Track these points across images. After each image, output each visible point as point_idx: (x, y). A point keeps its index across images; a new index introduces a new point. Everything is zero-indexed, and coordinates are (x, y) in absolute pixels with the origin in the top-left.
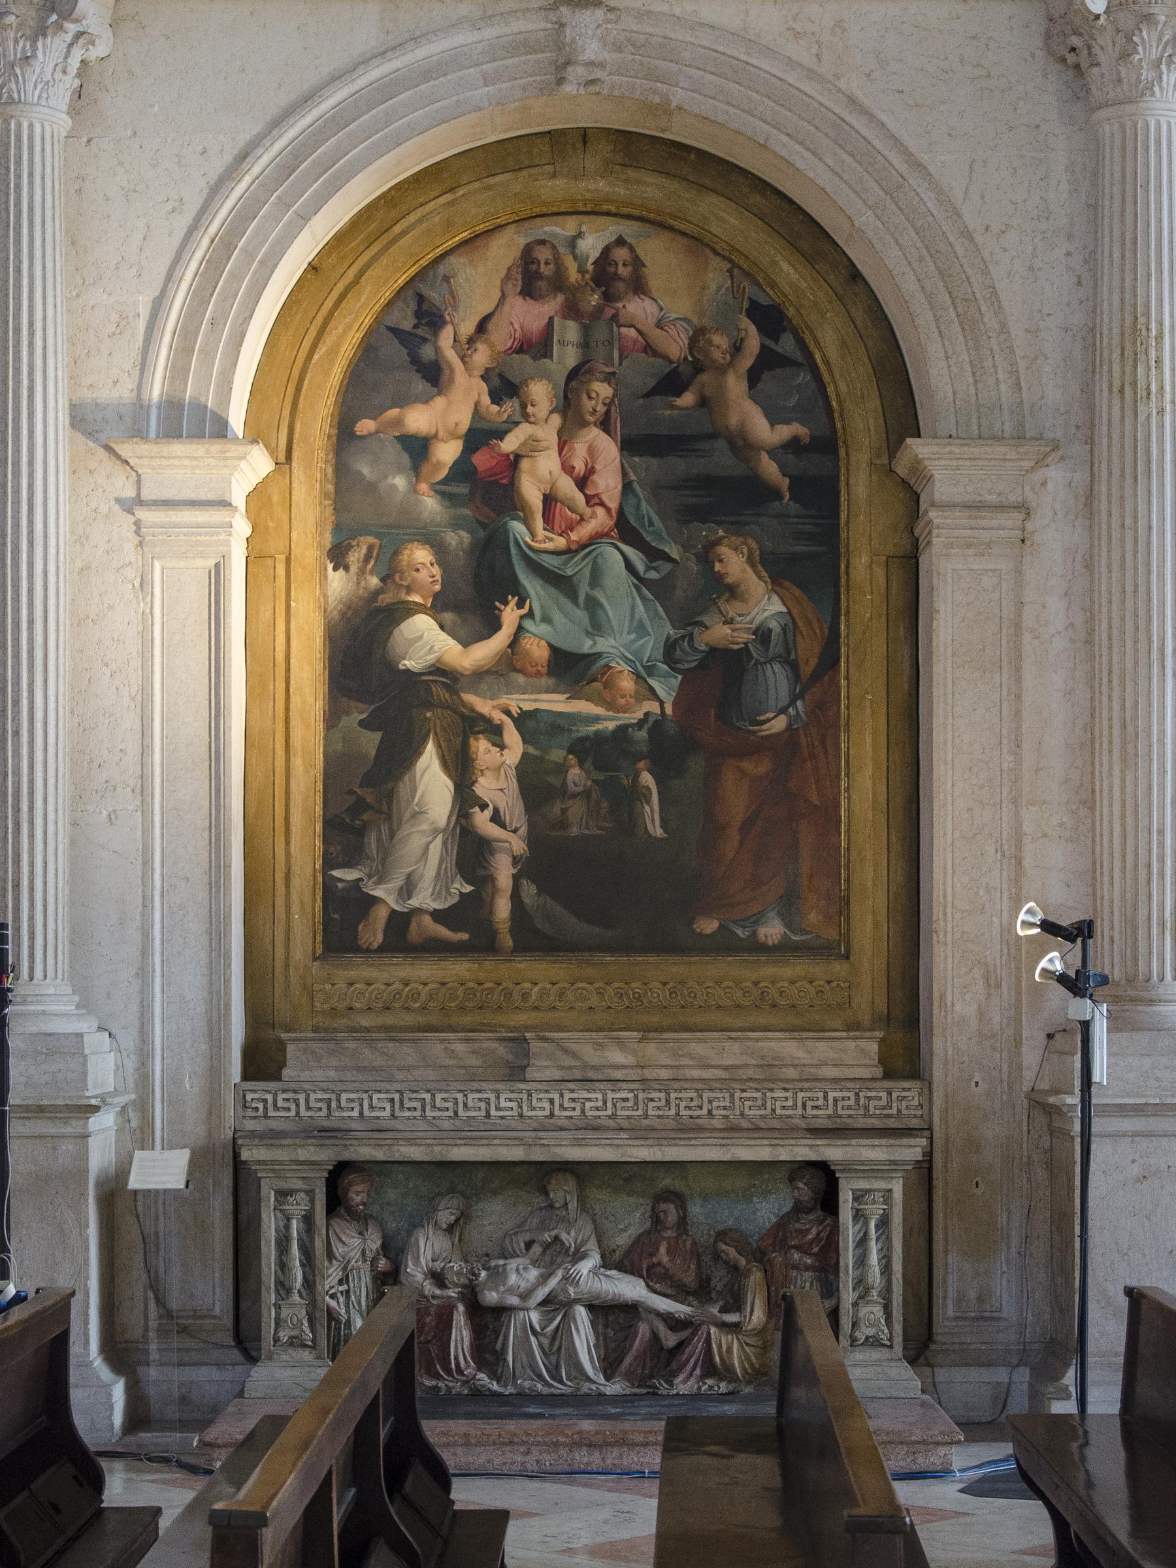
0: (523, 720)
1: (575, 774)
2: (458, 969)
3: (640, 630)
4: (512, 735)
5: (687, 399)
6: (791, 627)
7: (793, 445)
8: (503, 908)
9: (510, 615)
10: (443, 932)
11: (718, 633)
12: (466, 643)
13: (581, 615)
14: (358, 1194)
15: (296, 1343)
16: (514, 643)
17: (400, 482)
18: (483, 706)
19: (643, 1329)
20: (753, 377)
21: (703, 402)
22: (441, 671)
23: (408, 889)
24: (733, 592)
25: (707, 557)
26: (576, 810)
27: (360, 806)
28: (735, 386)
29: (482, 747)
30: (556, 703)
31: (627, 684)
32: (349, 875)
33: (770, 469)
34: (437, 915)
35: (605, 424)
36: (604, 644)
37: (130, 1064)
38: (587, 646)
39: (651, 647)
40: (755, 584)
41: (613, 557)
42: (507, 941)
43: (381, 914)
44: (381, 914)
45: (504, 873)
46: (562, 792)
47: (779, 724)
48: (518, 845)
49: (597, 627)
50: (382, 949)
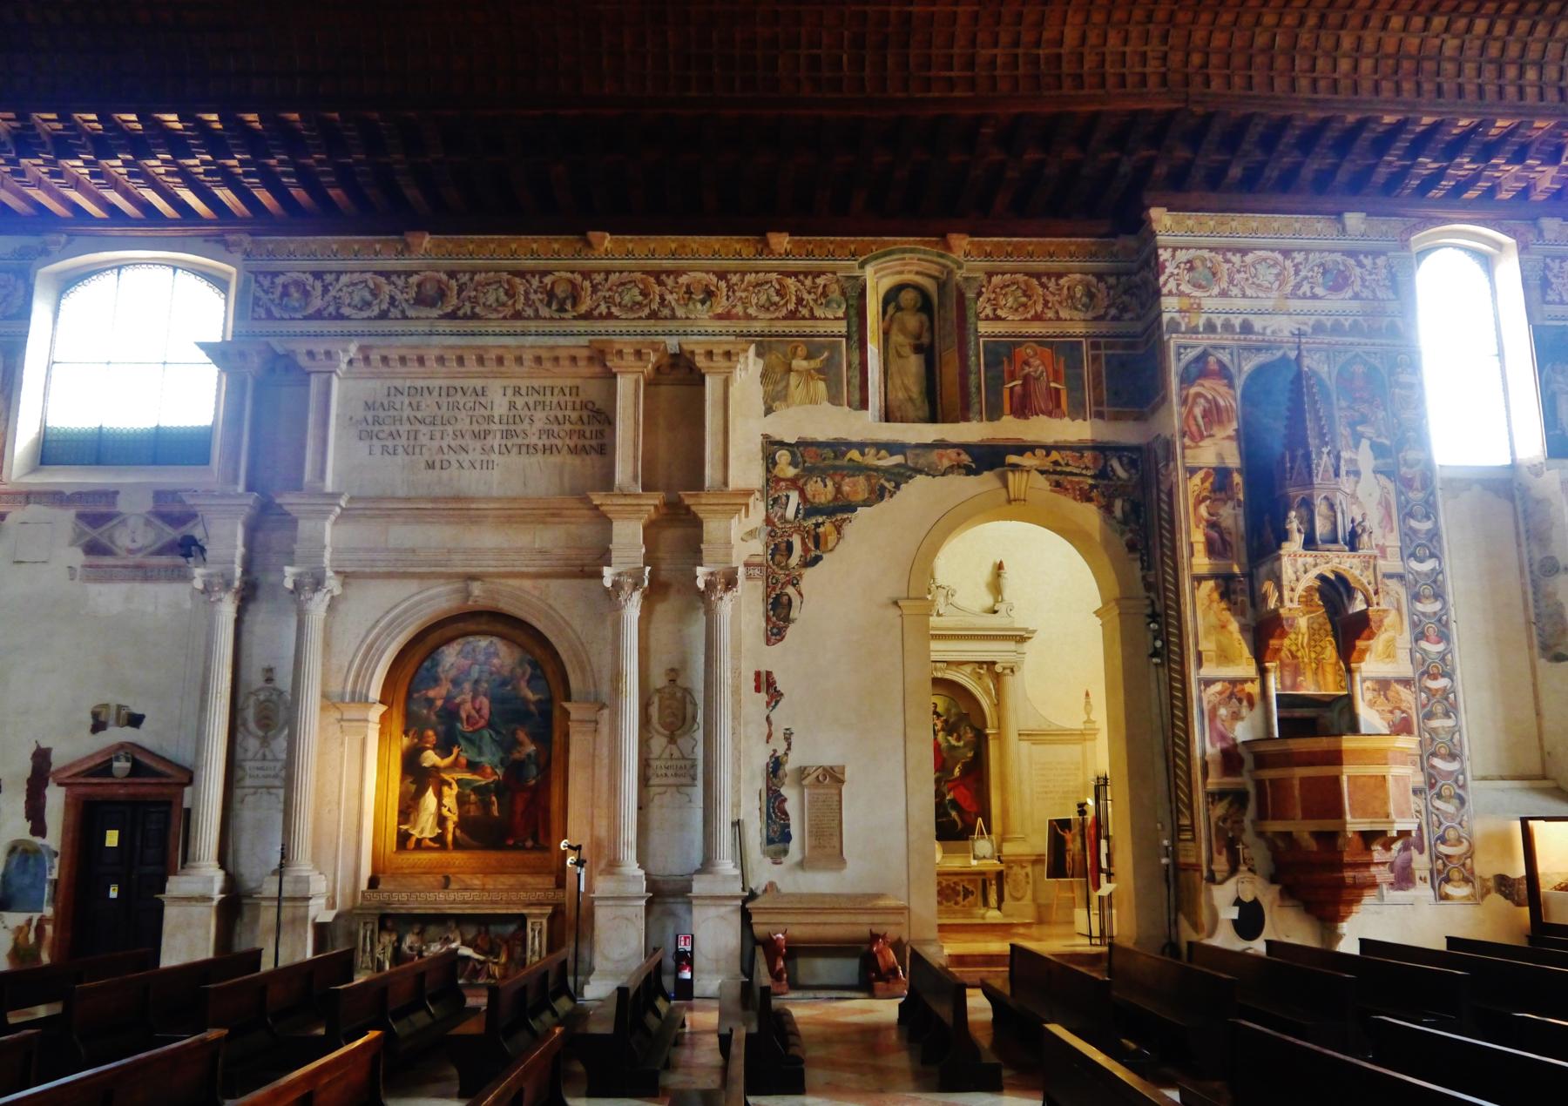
0: (459, 782)
1: (473, 797)
2: (435, 856)
3: (494, 755)
4: (455, 786)
5: (509, 688)
6: (537, 751)
7: (539, 702)
8: (450, 837)
9: (455, 751)
10: (431, 844)
11: (516, 756)
12: (443, 758)
13: (476, 750)
14: (389, 924)
15: (367, 968)
16: (457, 758)
17: (425, 711)
18: (447, 777)
19: (471, 964)
20: (529, 682)
21: (514, 688)
22: (435, 768)
23: (422, 831)
24: (521, 744)
25: (514, 733)
26: (472, 808)
27: (409, 807)
28: (523, 684)
29: (446, 789)
30: (468, 776)
31: (489, 770)
32: (404, 827)
33: (532, 708)
34: (431, 839)
35: (485, 695)
36: (483, 759)
37: (331, 885)
38: (478, 759)
39: (496, 759)
40: (526, 740)
41: (486, 733)
42: (450, 846)
43: (414, 839)
44: (414, 839)
45: (450, 826)
46: (469, 803)
47: (533, 782)
48: (455, 818)
49: (481, 753)
50: (415, 849)
